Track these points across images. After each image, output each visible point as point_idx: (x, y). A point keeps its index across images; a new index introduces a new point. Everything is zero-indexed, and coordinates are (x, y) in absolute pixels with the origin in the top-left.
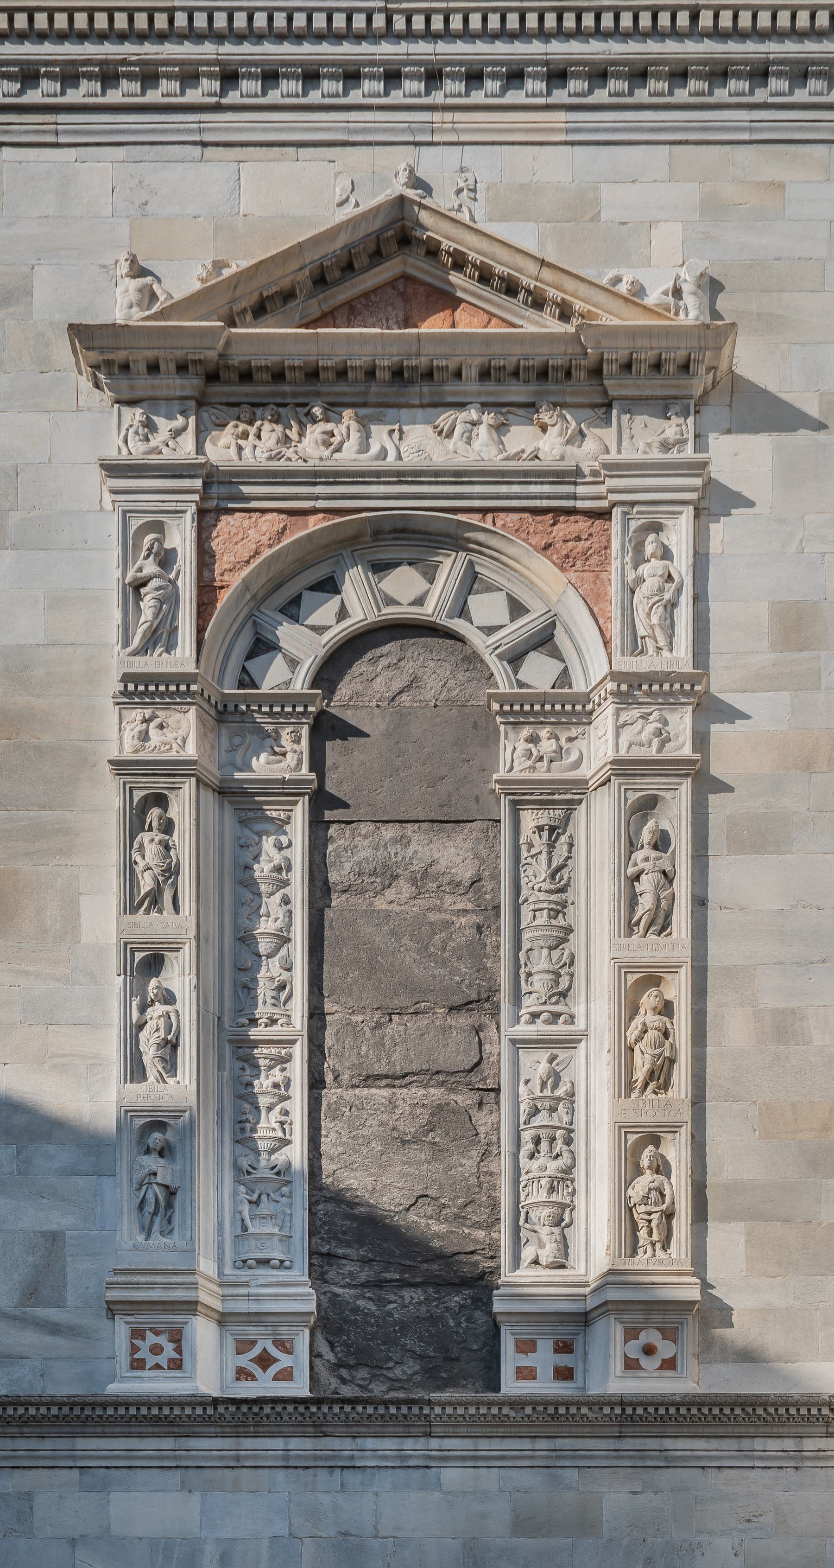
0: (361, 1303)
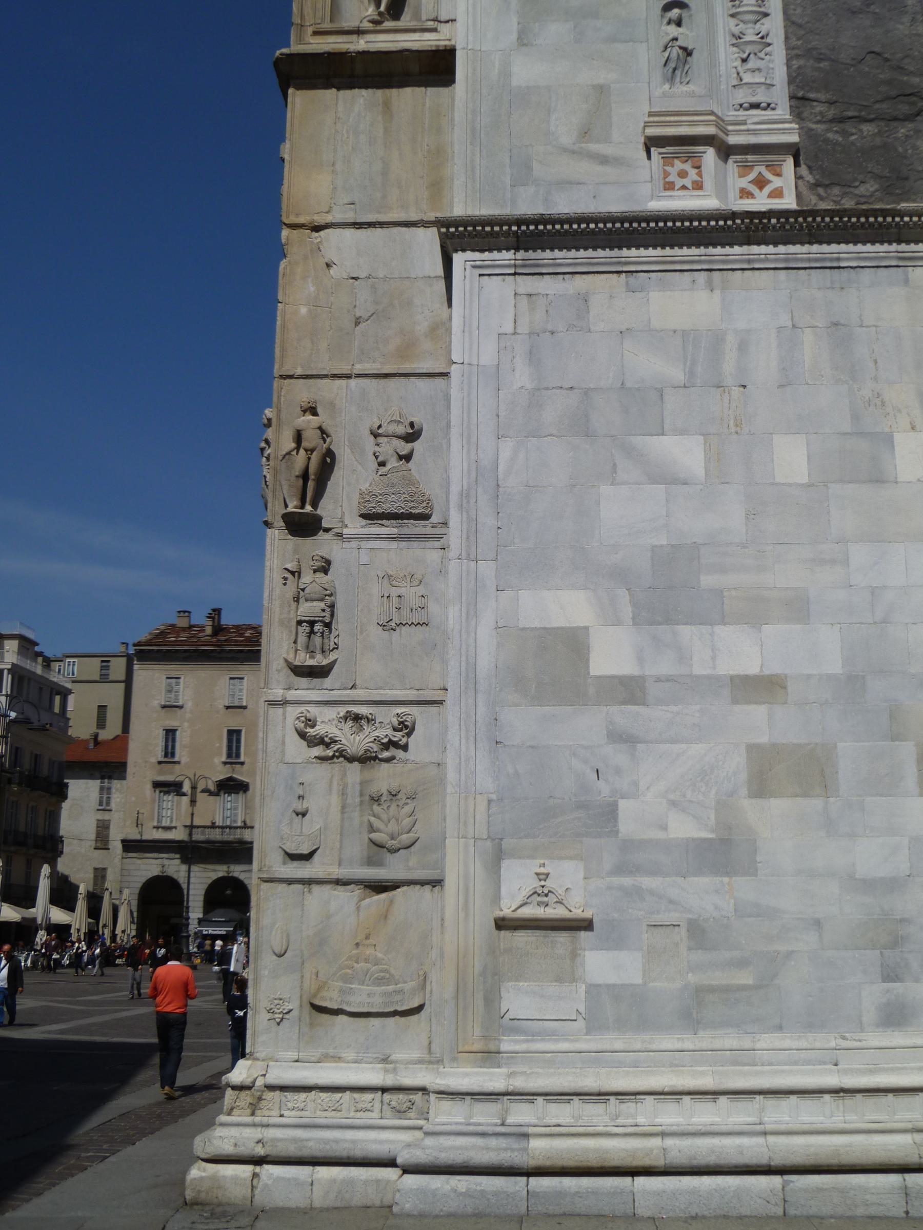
0: (830, 135)
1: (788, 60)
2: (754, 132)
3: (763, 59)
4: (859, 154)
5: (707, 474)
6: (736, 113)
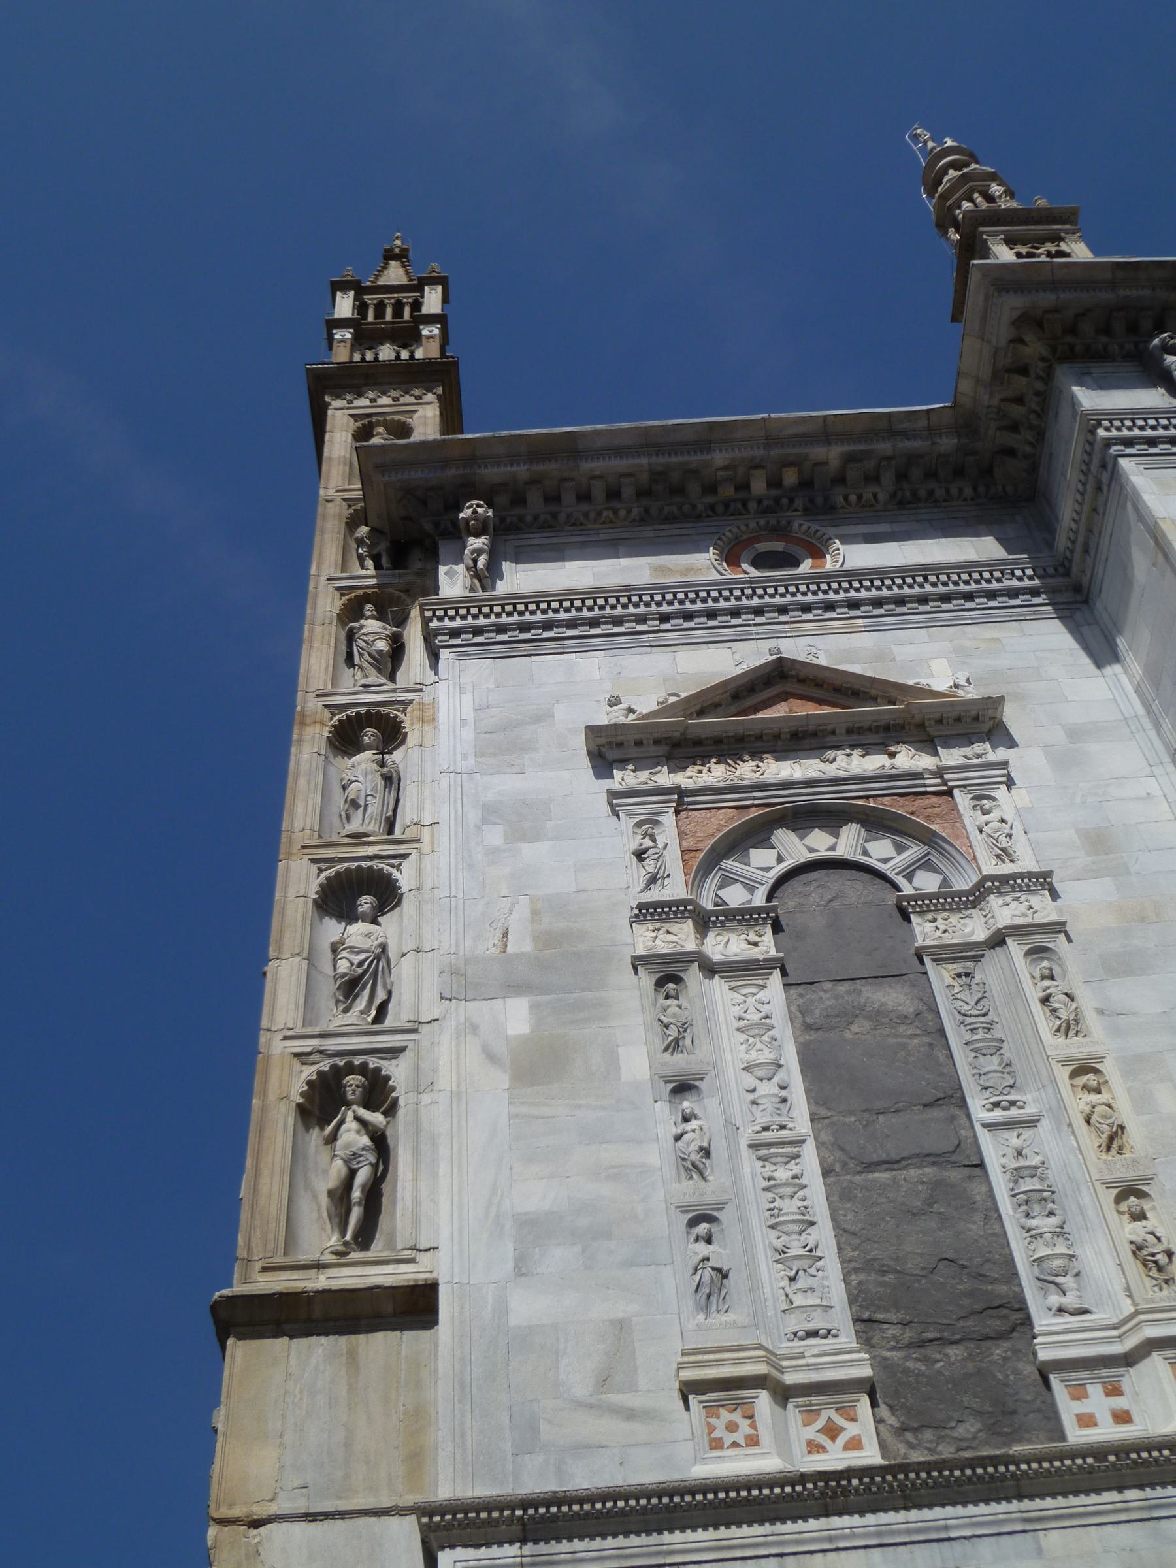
0: (910, 1364)
1: (845, 1275)
2: (815, 1367)
3: (815, 1276)
4: (950, 1386)
6: (791, 1344)
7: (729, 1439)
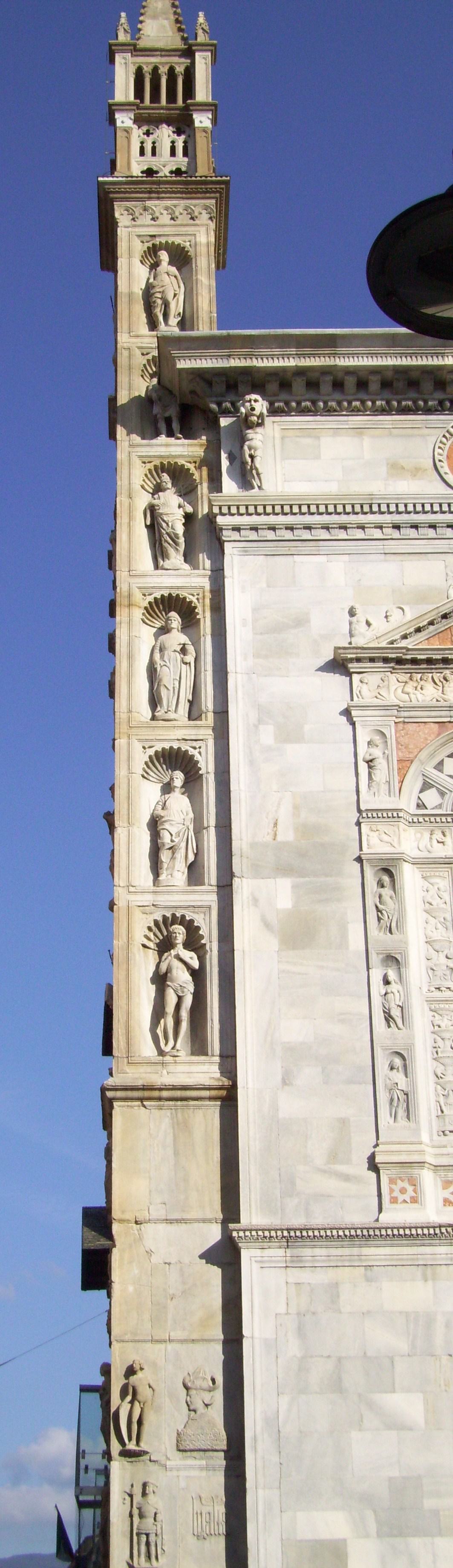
5: (426, 1423)
7: (401, 1198)
